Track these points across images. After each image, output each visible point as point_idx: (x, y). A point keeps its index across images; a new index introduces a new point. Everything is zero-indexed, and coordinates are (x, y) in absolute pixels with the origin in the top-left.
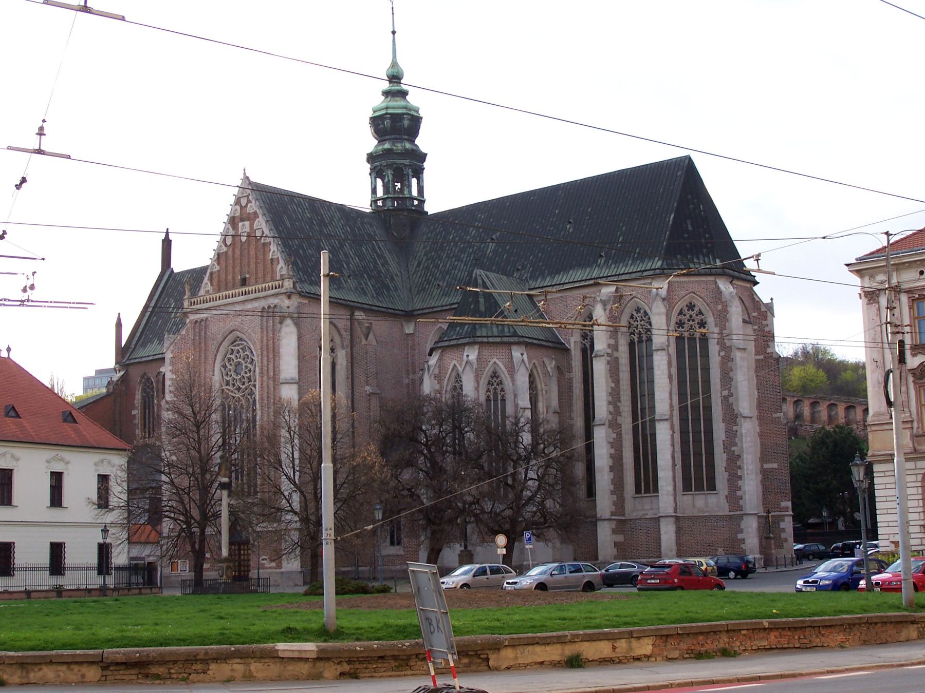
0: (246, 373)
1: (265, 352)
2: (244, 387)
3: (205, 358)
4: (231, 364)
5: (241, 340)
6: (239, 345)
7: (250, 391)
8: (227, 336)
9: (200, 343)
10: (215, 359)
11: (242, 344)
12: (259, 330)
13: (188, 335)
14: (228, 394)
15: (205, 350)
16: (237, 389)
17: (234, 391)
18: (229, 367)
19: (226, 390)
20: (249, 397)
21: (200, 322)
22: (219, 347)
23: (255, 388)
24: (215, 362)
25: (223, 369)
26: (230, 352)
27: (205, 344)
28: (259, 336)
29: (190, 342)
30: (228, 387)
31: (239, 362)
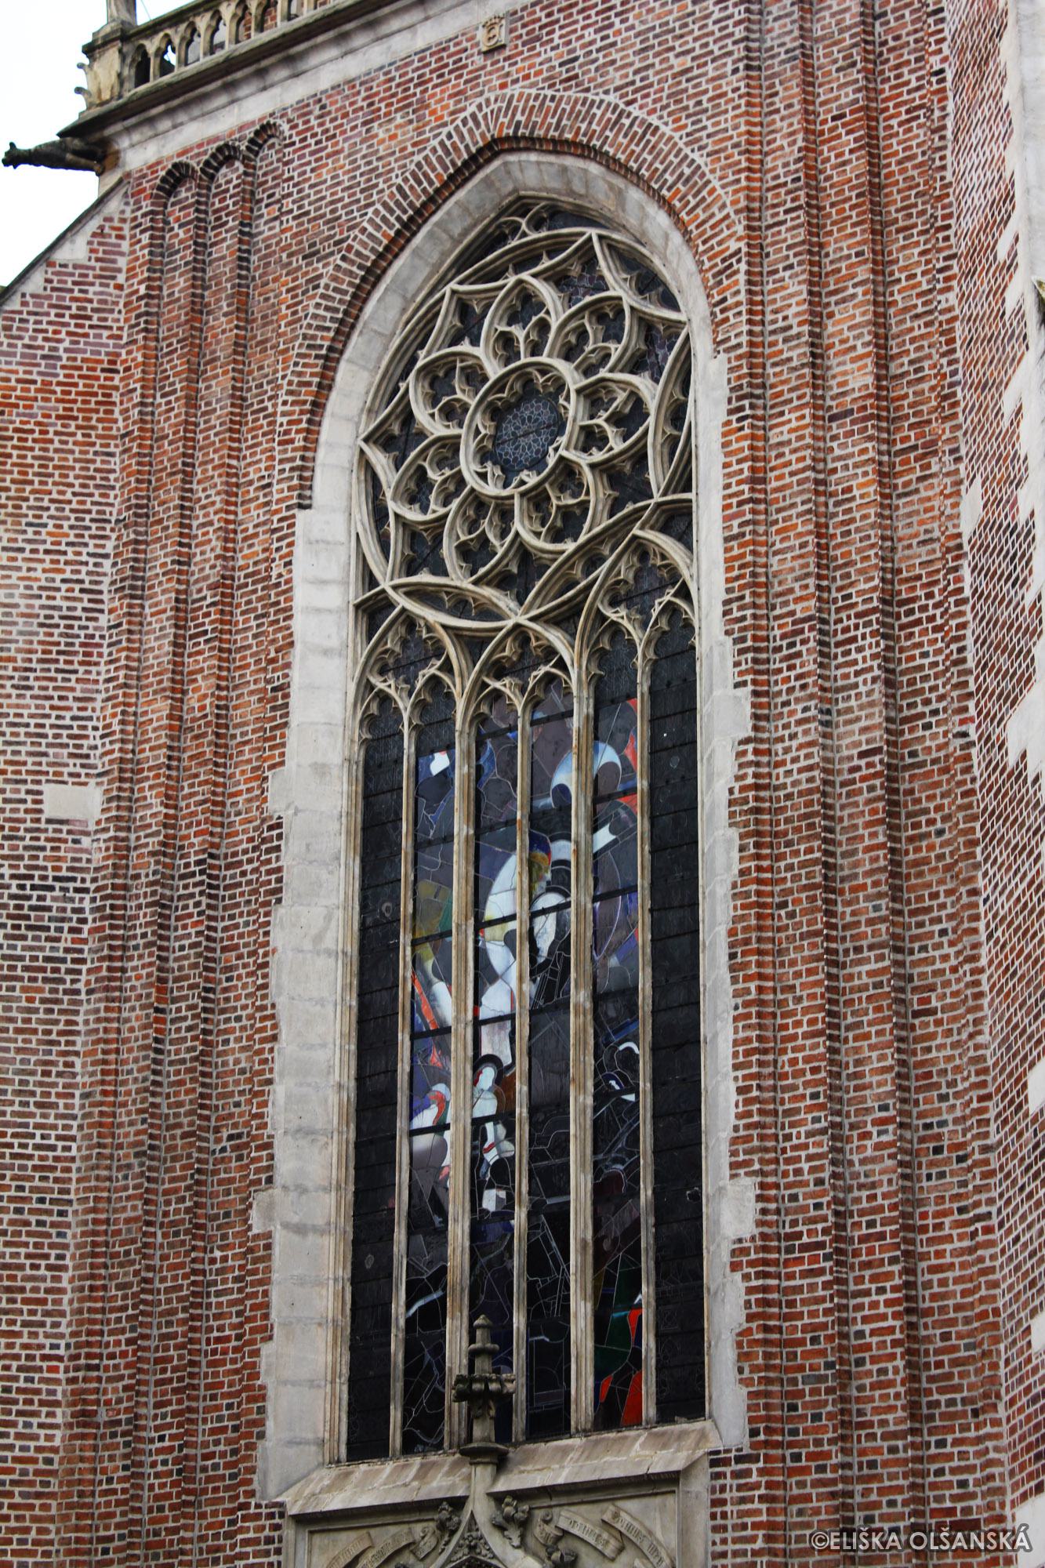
0: (591, 438)
1: (789, 235)
2: (569, 546)
3: (238, 399)
4: (452, 413)
5: (553, 213)
6: (526, 259)
7: (625, 572)
8: (434, 201)
9: (198, 309)
10: (325, 386)
11: (555, 246)
12: (734, 82)
13: (108, 275)
14: (409, 621)
15: (239, 347)
16: (502, 581)
17: (488, 592)
18: (437, 428)
19: (402, 601)
20: (618, 615)
21: (212, 167)
22: (360, 297)
23: (685, 537)
24: (318, 407)
25: (380, 460)
26: (446, 319)
27: (242, 308)
28: (732, 124)
29: (118, 319)
30: (424, 577)
31: (523, 375)
